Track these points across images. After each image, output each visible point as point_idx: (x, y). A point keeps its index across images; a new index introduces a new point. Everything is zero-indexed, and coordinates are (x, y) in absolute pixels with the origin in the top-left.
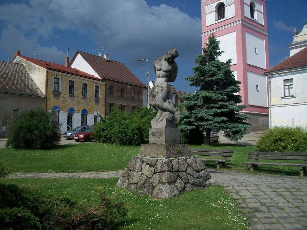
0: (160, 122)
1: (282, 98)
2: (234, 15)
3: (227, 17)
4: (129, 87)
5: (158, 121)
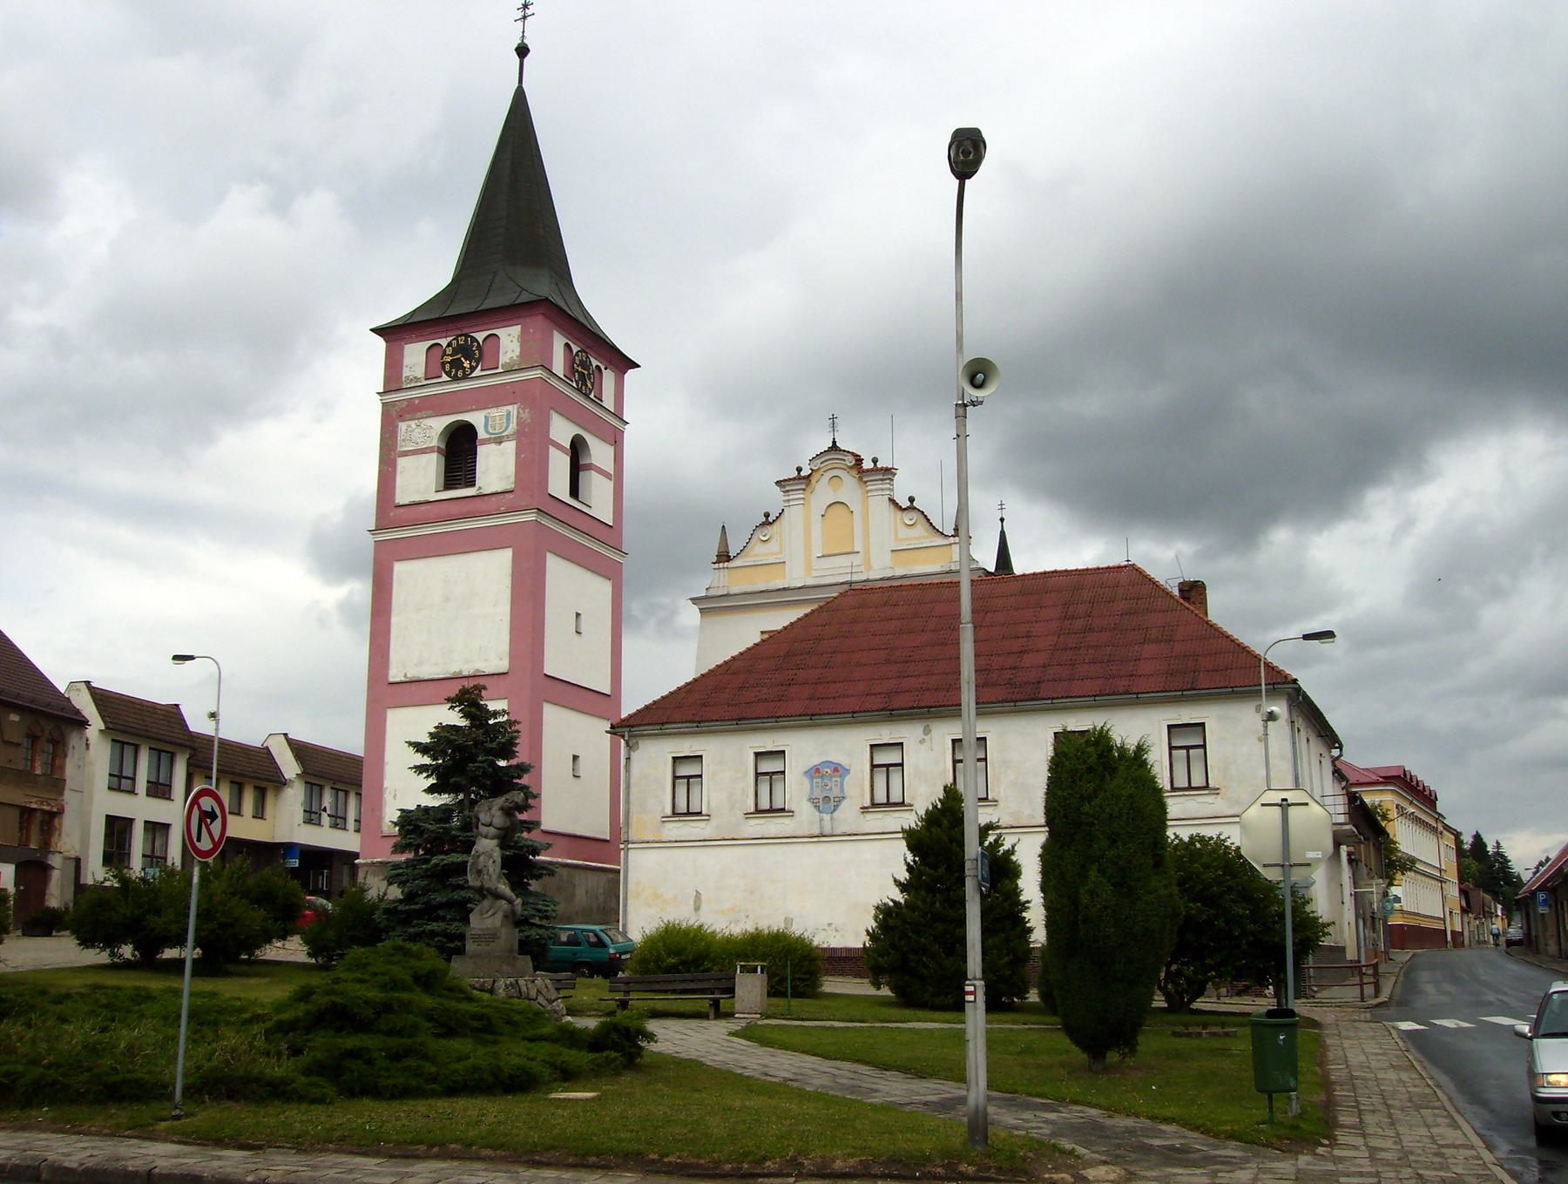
0: (490, 916)
1: (665, 819)
2: (510, 485)
3: (481, 485)
4: (15, 718)
5: (485, 916)
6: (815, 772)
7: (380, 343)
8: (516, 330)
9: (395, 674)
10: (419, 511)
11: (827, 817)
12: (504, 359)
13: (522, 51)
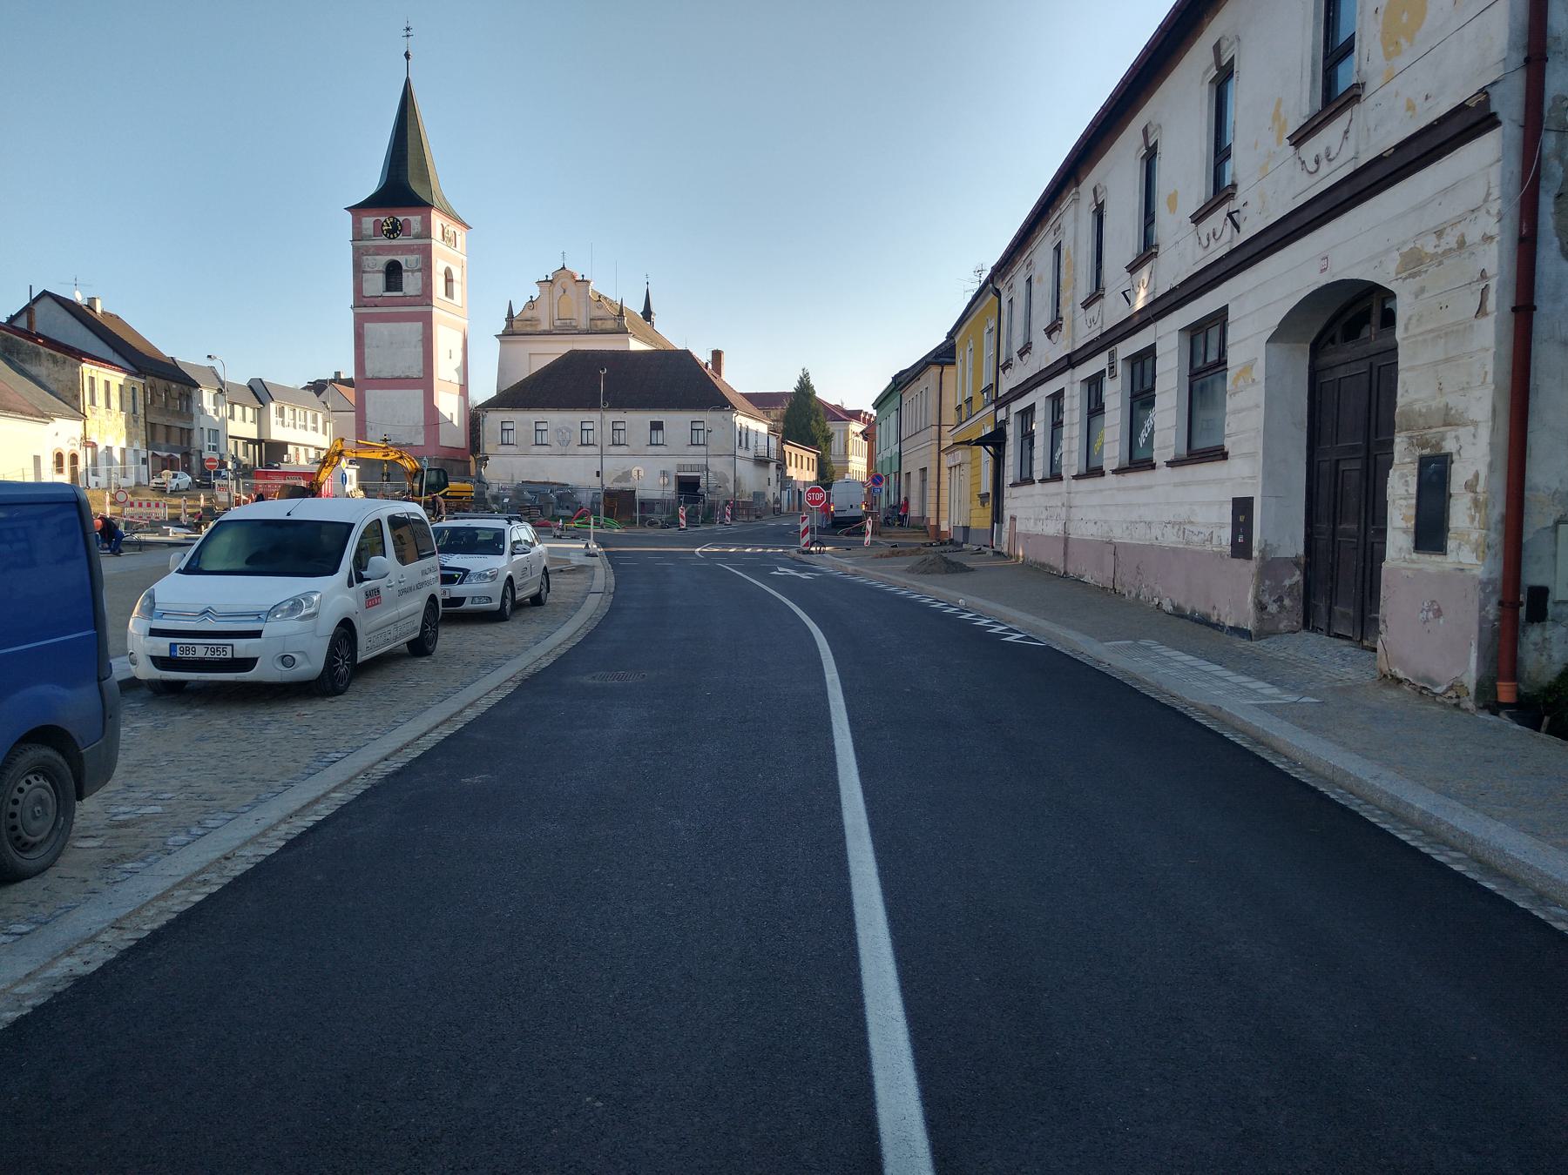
4: (174, 386)
6: (558, 430)
7: (349, 215)
8: (418, 218)
9: (369, 374)
10: (373, 302)
11: (564, 448)
12: (413, 232)
13: (407, 56)
